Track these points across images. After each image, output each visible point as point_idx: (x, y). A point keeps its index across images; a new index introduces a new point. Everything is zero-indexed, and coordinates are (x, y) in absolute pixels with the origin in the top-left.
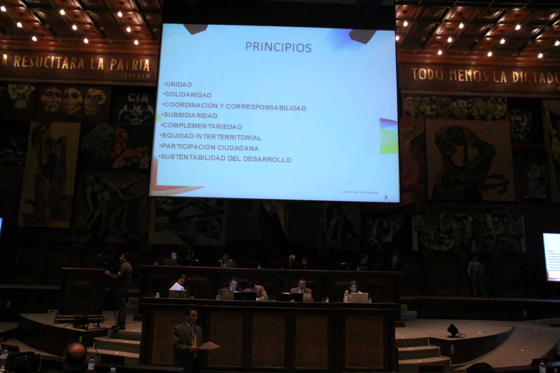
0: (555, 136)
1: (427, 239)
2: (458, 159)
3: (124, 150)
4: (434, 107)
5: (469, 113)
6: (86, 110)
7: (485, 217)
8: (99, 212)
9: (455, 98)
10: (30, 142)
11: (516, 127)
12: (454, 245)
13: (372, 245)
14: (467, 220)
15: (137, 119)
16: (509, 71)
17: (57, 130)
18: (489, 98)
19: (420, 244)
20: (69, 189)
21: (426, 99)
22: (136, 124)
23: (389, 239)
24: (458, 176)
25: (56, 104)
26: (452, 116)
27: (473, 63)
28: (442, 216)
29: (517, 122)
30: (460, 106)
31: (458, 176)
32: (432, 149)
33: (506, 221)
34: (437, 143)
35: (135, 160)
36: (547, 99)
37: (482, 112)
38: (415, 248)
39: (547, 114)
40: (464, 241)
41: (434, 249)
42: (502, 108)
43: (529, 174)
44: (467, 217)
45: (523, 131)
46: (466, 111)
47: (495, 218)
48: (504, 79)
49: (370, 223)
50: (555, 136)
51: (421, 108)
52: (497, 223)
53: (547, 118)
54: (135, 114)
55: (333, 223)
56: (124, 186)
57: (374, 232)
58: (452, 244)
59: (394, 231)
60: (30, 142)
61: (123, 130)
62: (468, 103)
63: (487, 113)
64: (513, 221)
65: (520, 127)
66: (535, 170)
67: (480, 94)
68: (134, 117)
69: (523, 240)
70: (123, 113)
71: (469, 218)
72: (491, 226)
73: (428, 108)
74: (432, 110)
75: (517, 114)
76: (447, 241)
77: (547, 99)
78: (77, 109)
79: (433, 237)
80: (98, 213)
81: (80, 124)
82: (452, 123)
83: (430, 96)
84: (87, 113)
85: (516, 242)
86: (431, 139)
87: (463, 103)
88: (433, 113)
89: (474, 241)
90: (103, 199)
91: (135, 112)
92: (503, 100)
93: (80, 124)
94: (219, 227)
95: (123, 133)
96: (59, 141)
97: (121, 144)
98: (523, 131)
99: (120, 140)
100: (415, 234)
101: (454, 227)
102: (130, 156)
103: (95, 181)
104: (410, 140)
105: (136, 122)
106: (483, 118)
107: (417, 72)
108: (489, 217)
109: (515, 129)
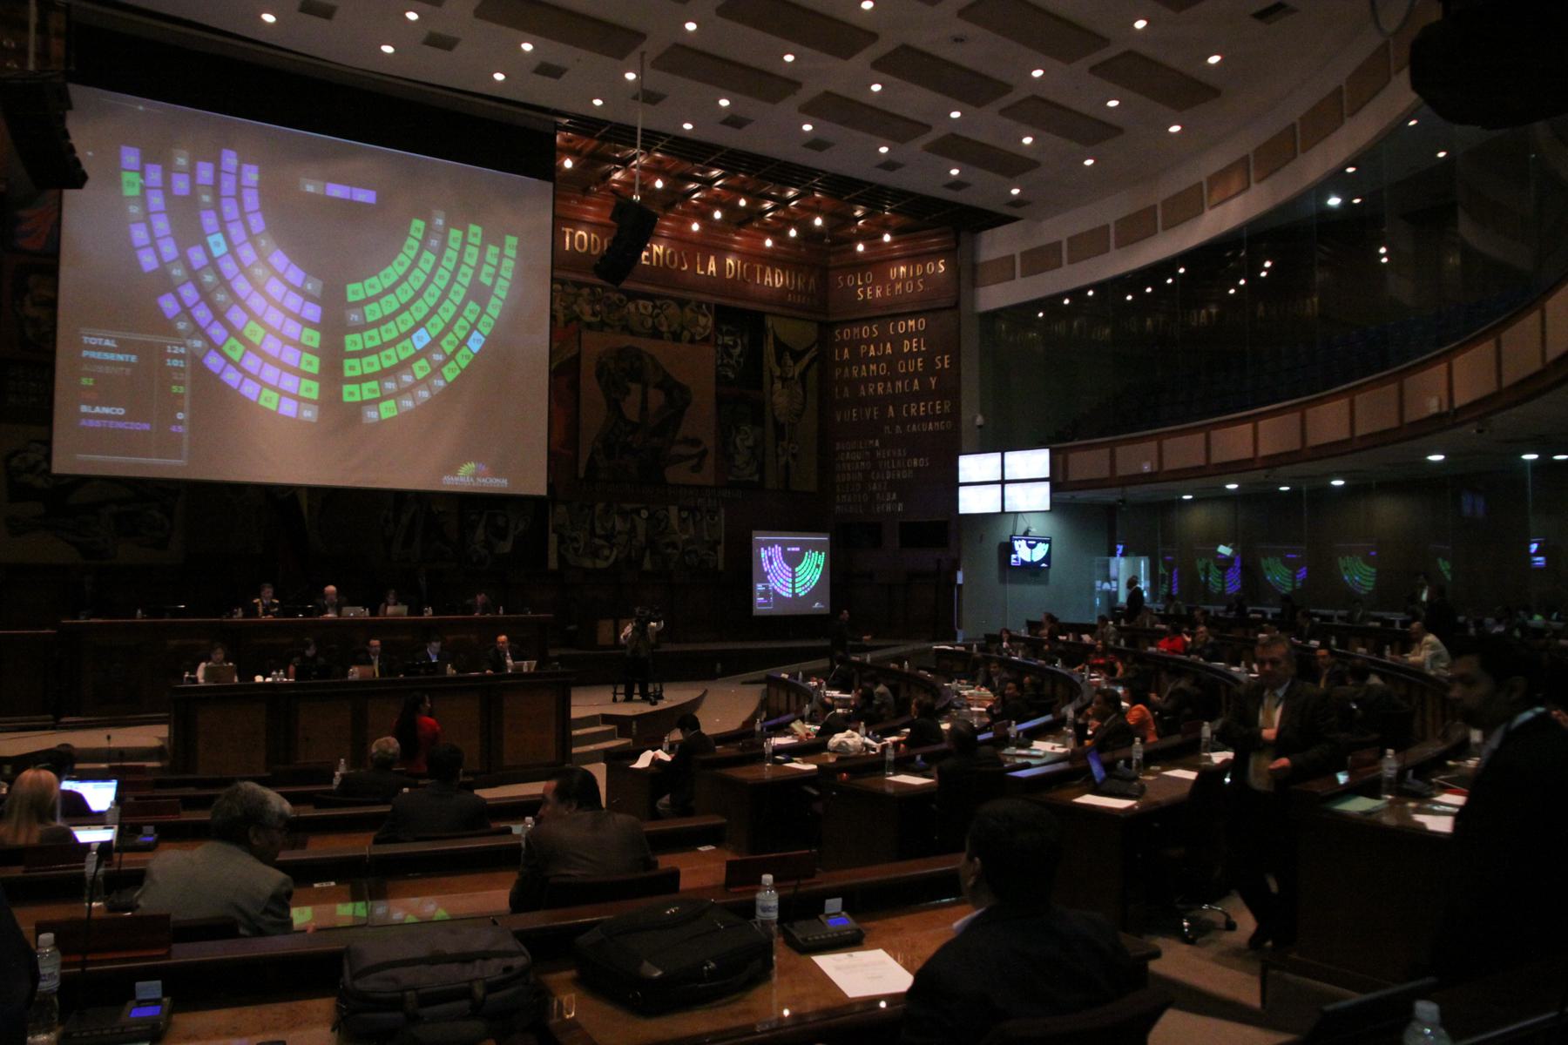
0: (780, 377)
2: (631, 409)
4: (598, 308)
5: (654, 327)
9: (633, 296)
16: (721, 252)
18: (688, 302)
19: (562, 559)
21: (586, 291)
23: (506, 547)
26: (627, 329)
27: (665, 233)
28: (600, 506)
29: (725, 346)
30: (642, 310)
32: (590, 386)
34: (599, 376)
36: (775, 314)
37: (675, 326)
38: (553, 564)
39: (771, 340)
42: (706, 321)
46: (649, 322)
48: (712, 267)
50: (780, 377)
51: (575, 307)
52: (684, 520)
53: (769, 348)
57: (480, 533)
62: (654, 307)
63: (683, 328)
65: (730, 356)
67: (676, 294)
69: (721, 548)
73: (587, 309)
74: (594, 314)
75: (728, 333)
76: (606, 552)
77: (775, 314)
82: (627, 341)
83: (592, 286)
86: (588, 366)
87: (645, 306)
88: (593, 319)
89: (648, 553)
92: (708, 308)
98: (733, 362)
100: (553, 539)
106: (676, 337)
107: (572, 235)
108: (674, 510)
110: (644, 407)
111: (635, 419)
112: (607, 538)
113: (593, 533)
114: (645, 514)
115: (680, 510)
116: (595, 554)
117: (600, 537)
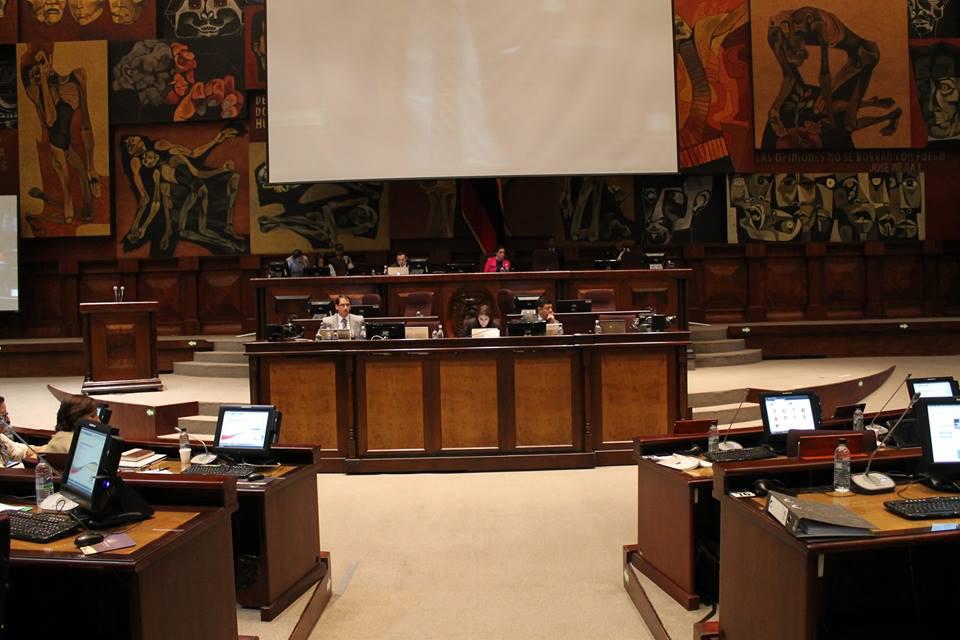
1: (754, 222)
2: (810, 73)
3: (190, 85)
6: (113, 14)
7: (856, 177)
8: (159, 204)
10: (20, 85)
11: (920, 7)
12: (801, 230)
13: (654, 236)
14: (825, 184)
15: (209, 25)
17: (66, 57)
19: (741, 231)
20: (101, 166)
22: (209, 35)
23: (684, 224)
24: (810, 104)
25: (56, 7)
28: (780, 178)
31: (810, 104)
33: (892, 185)
34: (772, 43)
35: (212, 104)
38: (733, 237)
40: (819, 223)
41: (766, 239)
43: (939, 97)
44: (826, 178)
45: (932, 13)
47: (874, 180)
49: (651, 196)
52: (877, 188)
54: (204, 15)
55: (582, 199)
56: (198, 153)
57: (658, 211)
58: (797, 230)
59: (695, 209)
60: (20, 85)
61: (185, 47)
64: (905, 183)
66: (950, 87)
68: (204, 22)
69: (921, 217)
70: (181, 16)
71: (829, 180)
72: (868, 196)
76: (790, 224)
78: (97, 15)
79: (763, 216)
80: (156, 206)
81: (105, 43)
84: (116, 20)
85: (909, 221)
89: (836, 222)
90: (162, 180)
91: (205, 12)
93: (105, 43)
94: (375, 214)
95: (185, 54)
96: (73, 77)
97: (184, 74)
98: (932, 13)
99: (181, 67)
100: (732, 212)
101: (802, 199)
102: (203, 96)
103: (145, 148)
104: (721, 39)
105: (209, 31)
109: (917, 10)
110: (825, 71)
111: (818, 85)
112: (792, 209)
113: (774, 205)
114: (831, 183)
115: (870, 178)
116: (778, 226)
117: (784, 209)
